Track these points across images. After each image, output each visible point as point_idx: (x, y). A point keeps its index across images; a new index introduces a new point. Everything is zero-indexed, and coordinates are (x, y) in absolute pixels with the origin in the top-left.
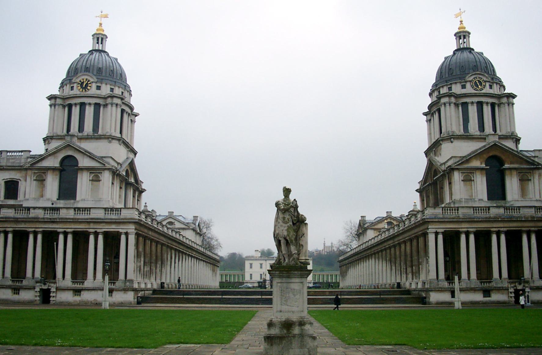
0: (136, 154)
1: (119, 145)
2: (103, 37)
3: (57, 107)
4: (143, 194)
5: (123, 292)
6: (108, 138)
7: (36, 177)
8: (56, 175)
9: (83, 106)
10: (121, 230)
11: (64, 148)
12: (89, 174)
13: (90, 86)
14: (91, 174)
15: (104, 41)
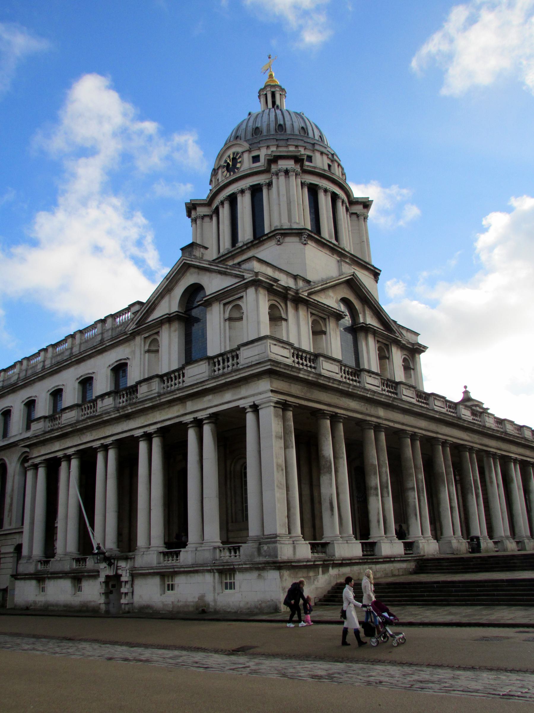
0: (379, 274)
1: (302, 246)
2: (273, 90)
3: (198, 222)
4: (422, 355)
5: (255, 574)
6: (274, 236)
7: (150, 346)
8: (175, 331)
9: (232, 200)
10: (242, 403)
11: (183, 275)
12: (222, 306)
13: (240, 162)
14: (227, 307)
15: (278, 96)
